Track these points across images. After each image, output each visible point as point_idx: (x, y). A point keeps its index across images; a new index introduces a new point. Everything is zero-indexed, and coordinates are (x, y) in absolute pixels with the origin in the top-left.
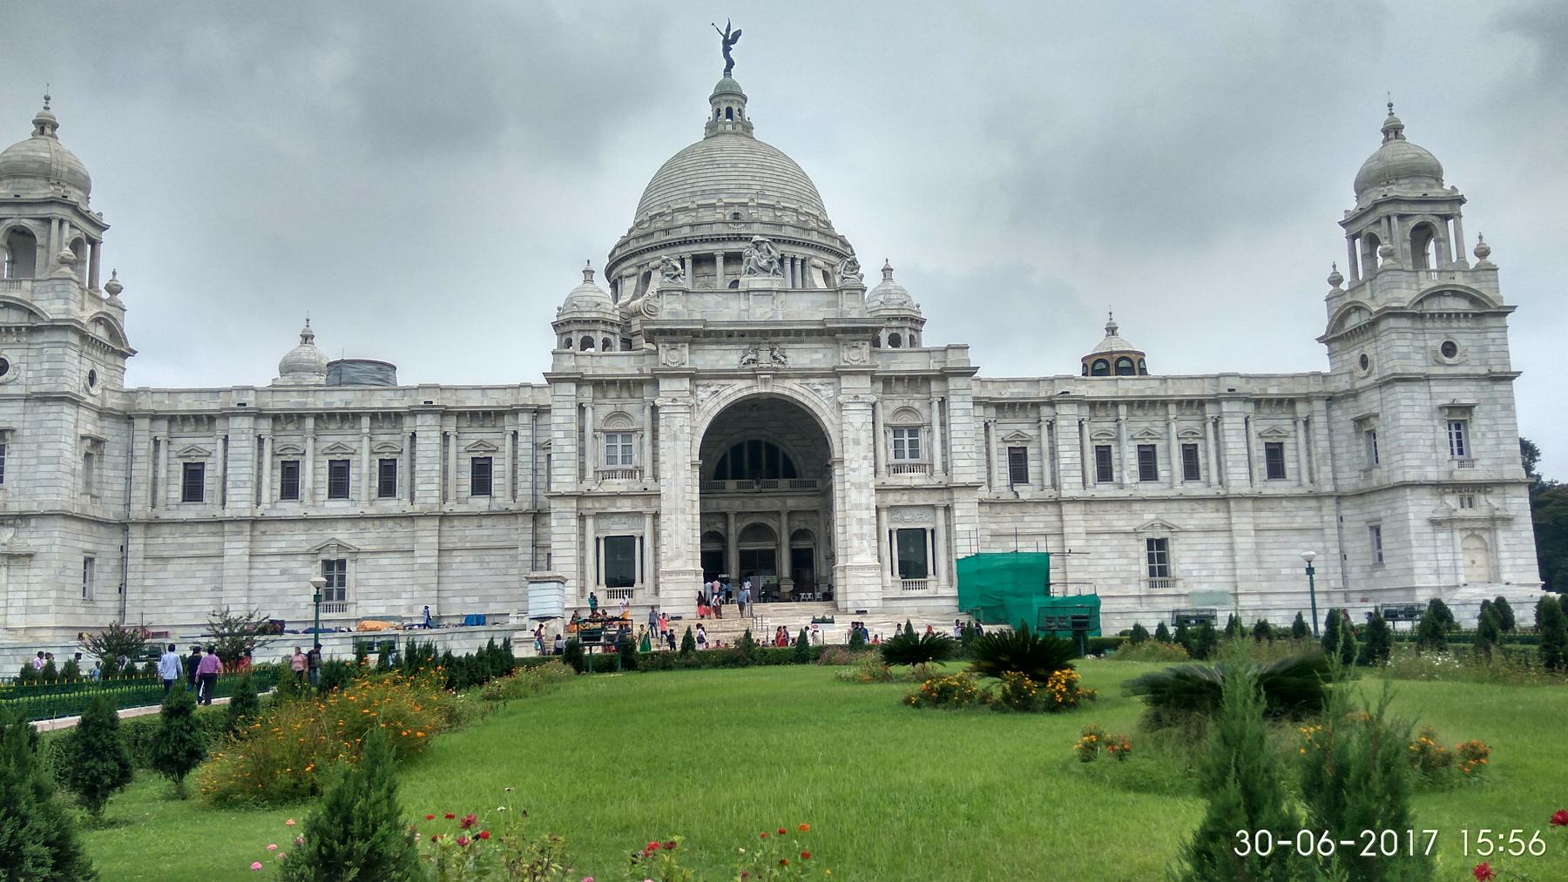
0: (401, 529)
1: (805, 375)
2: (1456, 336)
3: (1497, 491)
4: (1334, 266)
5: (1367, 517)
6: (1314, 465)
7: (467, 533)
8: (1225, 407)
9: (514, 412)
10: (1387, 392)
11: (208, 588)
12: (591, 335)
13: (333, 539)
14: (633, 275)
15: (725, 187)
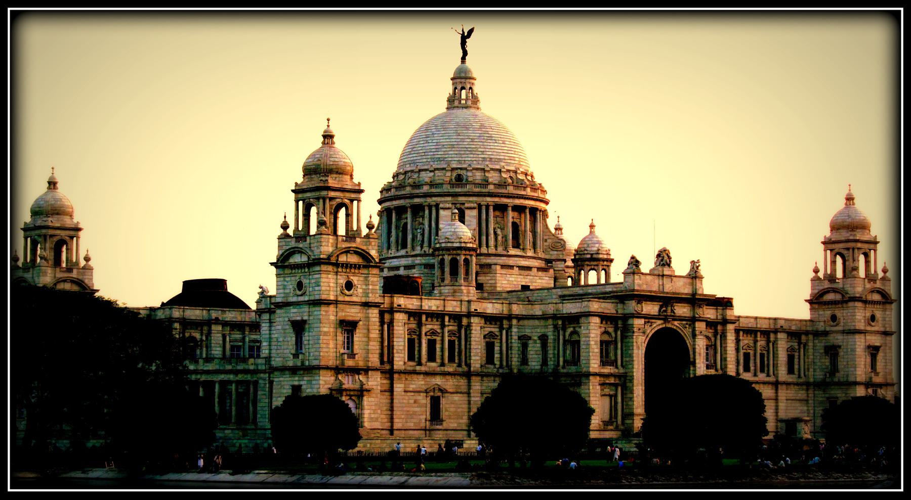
0: (462, 381)
1: (681, 319)
2: (875, 312)
3: (884, 388)
4: (816, 263)
5: (827, 395)
6: (806, 367)
7: (490, 384)
8: (781, 336)
9: (510, 317)
10: (850, 336)
11: (385, 408)
12: (468, 257)
13: (437, 385)
14: (449, 208)
15: (502, 157)
